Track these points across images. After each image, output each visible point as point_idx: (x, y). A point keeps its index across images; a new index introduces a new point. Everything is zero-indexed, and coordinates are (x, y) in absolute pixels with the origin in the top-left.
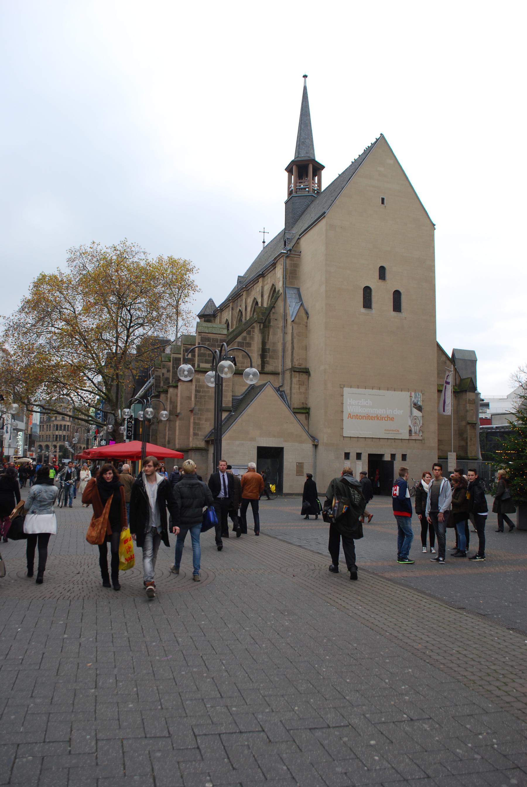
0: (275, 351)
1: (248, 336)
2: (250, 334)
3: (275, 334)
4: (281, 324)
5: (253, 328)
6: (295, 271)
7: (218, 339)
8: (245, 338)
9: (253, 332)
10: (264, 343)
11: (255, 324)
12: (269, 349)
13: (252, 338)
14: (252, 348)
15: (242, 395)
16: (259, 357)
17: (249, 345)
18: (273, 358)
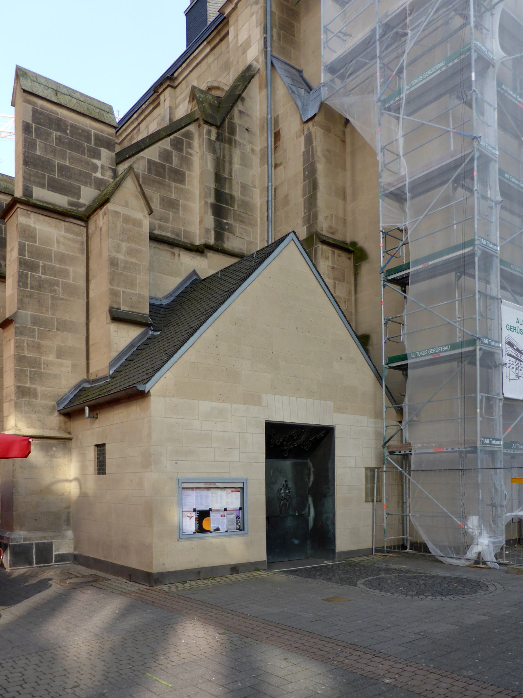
0: (246, 205)
1: (174, 152)
2: (180, 150)
3: (245, 162)
4: (260, 141)
5: (189, 135)
6: (292, 26)
7: (89, 133)
8: (166, 156)
9: (190, 146)
10: (221, 178)
11: (192, 128)
12: (232, 197)
13: (186, 161)
14: (186, 187)
15: (166, 297)
16: (210, 211)
17: (179, 176)
18: (242, 222)
